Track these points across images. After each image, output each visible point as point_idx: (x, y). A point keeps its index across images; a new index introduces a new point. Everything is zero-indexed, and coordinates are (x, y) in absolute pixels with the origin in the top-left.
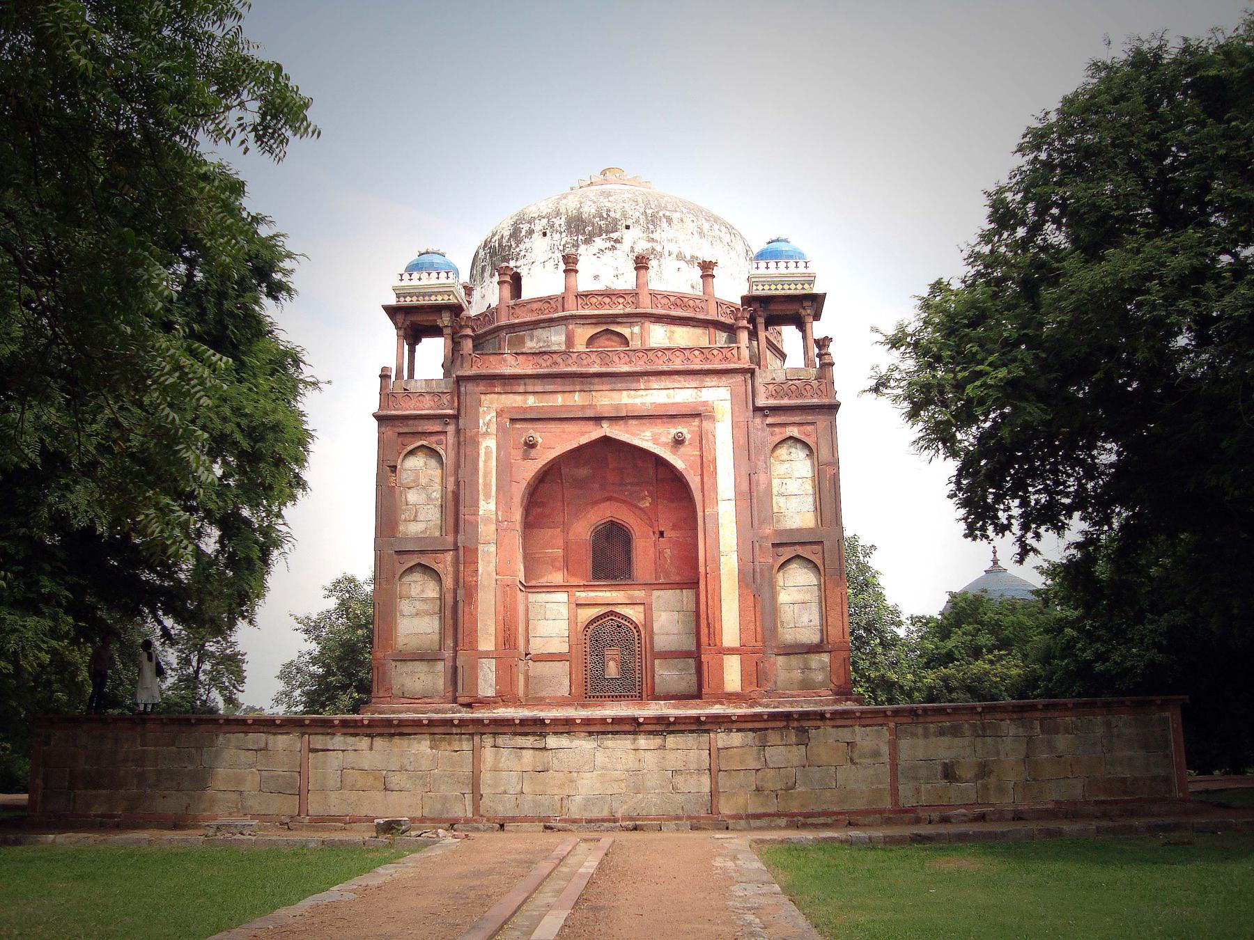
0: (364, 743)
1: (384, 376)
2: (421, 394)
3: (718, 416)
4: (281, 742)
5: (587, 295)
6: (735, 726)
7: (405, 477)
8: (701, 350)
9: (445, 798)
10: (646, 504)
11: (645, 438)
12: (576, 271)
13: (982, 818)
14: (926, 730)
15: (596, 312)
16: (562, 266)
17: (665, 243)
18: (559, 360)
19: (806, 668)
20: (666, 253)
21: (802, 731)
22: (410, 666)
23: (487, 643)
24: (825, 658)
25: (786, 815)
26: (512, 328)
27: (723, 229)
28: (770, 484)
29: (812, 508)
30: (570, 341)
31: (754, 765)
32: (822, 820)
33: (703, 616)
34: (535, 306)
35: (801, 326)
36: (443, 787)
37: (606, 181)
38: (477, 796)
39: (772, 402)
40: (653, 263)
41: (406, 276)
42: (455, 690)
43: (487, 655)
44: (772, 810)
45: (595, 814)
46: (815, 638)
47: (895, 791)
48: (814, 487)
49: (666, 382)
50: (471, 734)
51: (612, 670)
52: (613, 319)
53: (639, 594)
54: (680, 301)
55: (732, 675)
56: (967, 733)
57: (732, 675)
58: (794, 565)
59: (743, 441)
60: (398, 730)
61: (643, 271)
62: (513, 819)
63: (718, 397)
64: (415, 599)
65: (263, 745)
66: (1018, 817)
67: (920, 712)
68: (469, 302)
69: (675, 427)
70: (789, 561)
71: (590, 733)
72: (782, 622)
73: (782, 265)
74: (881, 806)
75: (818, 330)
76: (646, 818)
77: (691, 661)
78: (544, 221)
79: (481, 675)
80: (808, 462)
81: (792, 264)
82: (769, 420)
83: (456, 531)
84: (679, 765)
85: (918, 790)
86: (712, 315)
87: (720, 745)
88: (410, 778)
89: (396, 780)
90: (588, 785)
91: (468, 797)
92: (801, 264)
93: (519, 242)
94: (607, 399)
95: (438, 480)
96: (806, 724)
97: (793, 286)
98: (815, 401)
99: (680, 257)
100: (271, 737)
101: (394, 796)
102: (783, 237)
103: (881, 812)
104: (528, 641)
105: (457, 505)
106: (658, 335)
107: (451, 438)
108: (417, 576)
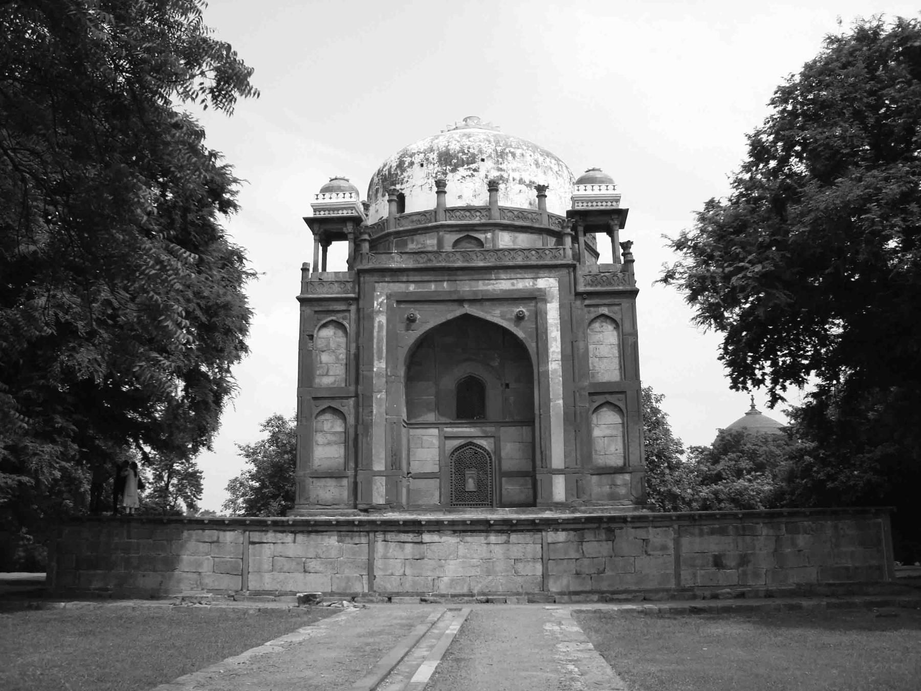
0: (289, 538)
1: (305, 269)
2: (332, 283)
4: (229, 537)
5: (453, 210)
6: (561, 527)
7: (320, 343)
8: (537, 250)
9: (348, 579)
10: (496, 363)
11: (495, 315)
12: (445, 192)
13: (742, 595)
14: (701, 530)
15: (459, 222)
16: (435, 189)
17: (510, 172)
18: (432, 258)
19: (614, 484)
20: (511, 179)
21: (610, 531)
22: (322, 482)
23: (379, 465)
24: (627, 477)
26: (398, 234)
27: (553, 161)
28: (587, 350)
29: (618, 367)
30: (440, 243)
31: (573, 555)
32: (623, 596)
33: (537, 446)
34: (415, 218)
35: (611, 233)
36: (347, 571)
37: (467, 126)
38: (372, 577)
39: (589, 289)
40: (502, 186)
41: (321, 196)
42: (356, 498)
43: (379, 473)
44: (588, 588)
45: (458, 590)
46: (620, 463)
47: (678, 575)
48: (619, 352)
50: (368, 532)
51: (471, 485)
53: (490, 429)
54: (521, 214)
55: (559, 489)
56: (731, 533)
57: (559, 489)
58: (605, 409)
59: (566, 318)
60: (315, 528)
61: (494, 193)
62: (398, 594)
63: (548, 283)
64: (327, 433)
65: (215, 539)
66: (769, 595)
68: (367, 215)
71: (455, 532)
72: (596, 451)
74: (668, 586)
75: (623, 235)
76: (495, 594)
77: (528, 478)
78: (422, 155)
79: (375, 488)
80: (615, 333)
82: (587, 302)
83: (357, 382)
84: (519, 555)
85: (695, 575)
86: (545, 224)
87: (550, 540)
88: (322, 564)
89: (313, 565)
91: (365, 578)
92: (611, 187)
93: (403, 171)
94: (467, 287)
95: (344, 345)
96: (613, 526)
98: (621, 288)
99: (521, 182)
100: (221, 533)
101: (310, 577)
103: (667, 590)
104: (409, 464)
105: (357, 364)
106: (505, 240)
107: (353, 315)
108: (328, 416)
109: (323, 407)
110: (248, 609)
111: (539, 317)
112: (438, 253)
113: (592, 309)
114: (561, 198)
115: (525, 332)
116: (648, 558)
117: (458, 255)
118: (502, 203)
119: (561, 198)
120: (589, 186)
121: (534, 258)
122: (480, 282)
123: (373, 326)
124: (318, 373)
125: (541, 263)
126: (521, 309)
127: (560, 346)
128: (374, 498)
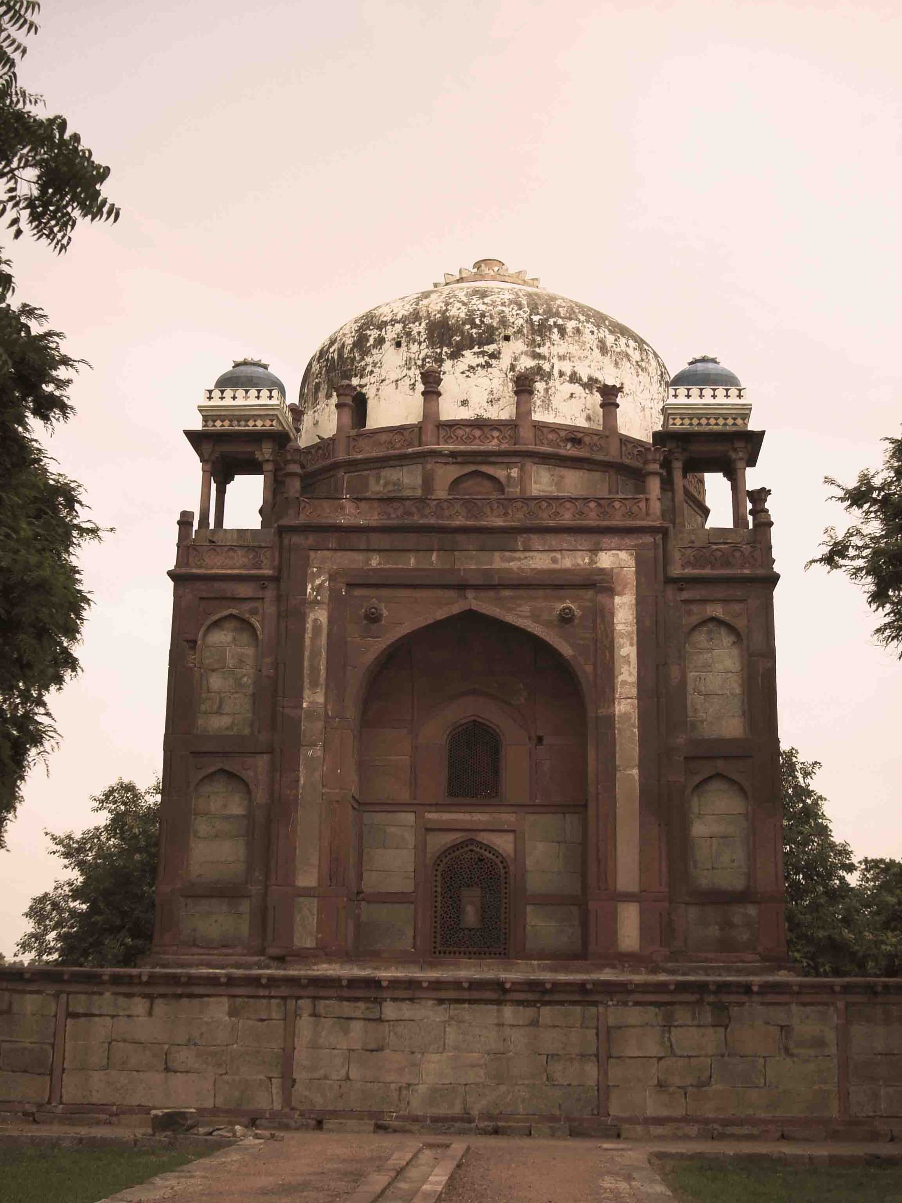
0: (139, 1006)
1: (185, 521)
2: (232, 548)
3: (619, 589)
4: (30, 1004)
5: (453, 425)
8: (597, 500)
11: (521, 615)
12: (439, 394)
15: (462, 448)
16: (420, 387)
17: (555, 360)
18: (414, 509)
20: (556, 372)
21: (721, 1009)
23: (307, 878)
24: (752, 910)
25: (697, 1121)
26: (352, 465)
27: (632, 343)
28: (683, 682)
30: (428, 483)
32: (745, 1130)
34: (384, 437)
38: (289, 1082)
39: (689, 571)
40: (540, 386)
41: (217, 394)
43: (307, 892)
44: (679, 1112)
45: (442, 1110)
46: (739, 884)
49: (552, 540)
51: (471, 916)
52: (486, 457)
53: (508, 818)
54: (574, 436)
55: (629, 927)
57: (629, 927)
58: (715, 785)
59: (648, 623)
61: (524, 397)
62: (334, 1114)
63: (616, 559)
65: (5, 1007)
67: (879, 989)
68: (298, 430)
69: (562, 599)
70: (705, 781)
71: (441, 1001)
73: (708, 392)
75: (753, 479)
77: (572, 908)
78: (399, 327)
79: (298, 918)
80: (735, 652)
81: (720, 392)
82: (685, 595)
86: (613, 453)
87: (611, 1022)
89: (184, 1057)
90: (435, 1069)
92: (733, 392)
93: (365, 352)
94: (472, 562)
95: (250, 661)
96: (726, 998)
97: (721, 421)
98: (746, 571)
99: (574, 378)
101: (177, 1080)
102: (711, 356)
104: (360, 876)
106: (542, 482)
107: (271, 609)
108: (219, 787)
109: (212, 769)
110: (59, 1138)
111: (602, 618)
112: (422, 501)
113: (695, 608)
114: (643, 409)
115: (572, 645)
116: (788, 1060)
117: (458, 506)
118: (538, 416)
119: (643, 409)
120: (695, 391)
121: (593, 515)
122: (497, 555)
123: (304, 630)
124: (203, 707)
125: (605, 523)
126: (568, 604)
127: (635, 672)
128: (296, 935)
